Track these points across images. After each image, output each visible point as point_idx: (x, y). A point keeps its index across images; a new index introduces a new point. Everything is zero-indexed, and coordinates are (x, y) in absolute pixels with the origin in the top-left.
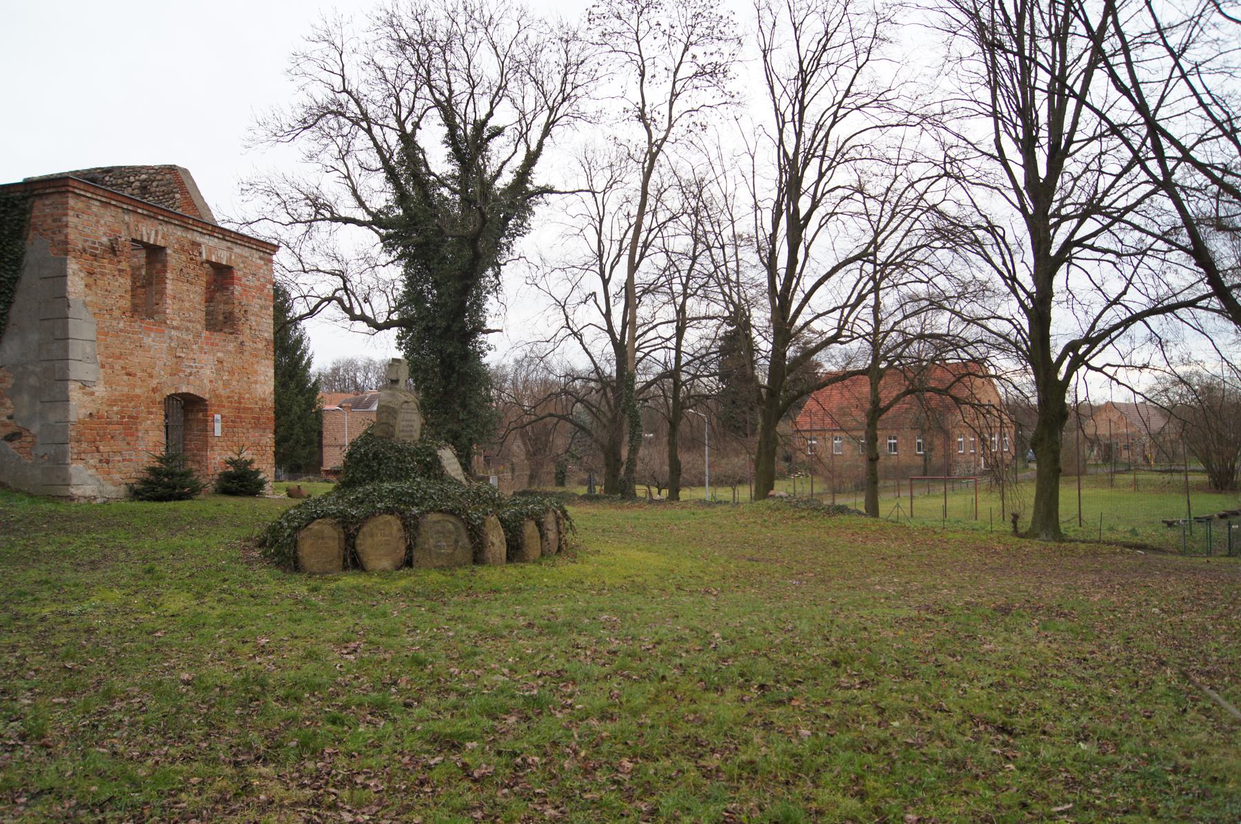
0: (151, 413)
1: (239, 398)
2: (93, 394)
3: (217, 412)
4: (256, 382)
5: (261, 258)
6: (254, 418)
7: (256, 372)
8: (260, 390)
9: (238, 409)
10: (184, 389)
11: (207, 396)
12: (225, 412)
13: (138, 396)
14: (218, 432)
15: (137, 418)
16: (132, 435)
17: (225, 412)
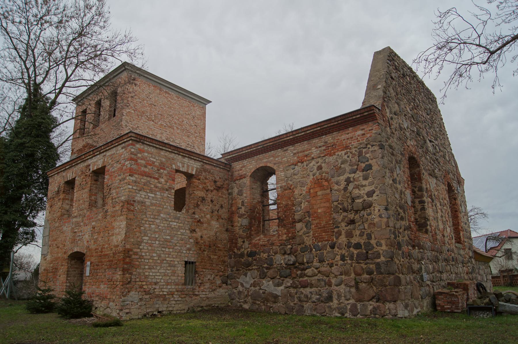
0: (62, 265)
1: (102, 249)
2: (46, 259)
3: (89, 260)
4: (113, 235)
5: (122, 148)
6: (109, 261)
7: (113, 228)
8: (115, 240)
9: (100, 256)
10: (76, 250)
11: (85, 252)
12: (93, 259)
13: (59, 257)
14: (87, 274)
15: (57, 269)
16: (55, 278)
17: (93, 259)
